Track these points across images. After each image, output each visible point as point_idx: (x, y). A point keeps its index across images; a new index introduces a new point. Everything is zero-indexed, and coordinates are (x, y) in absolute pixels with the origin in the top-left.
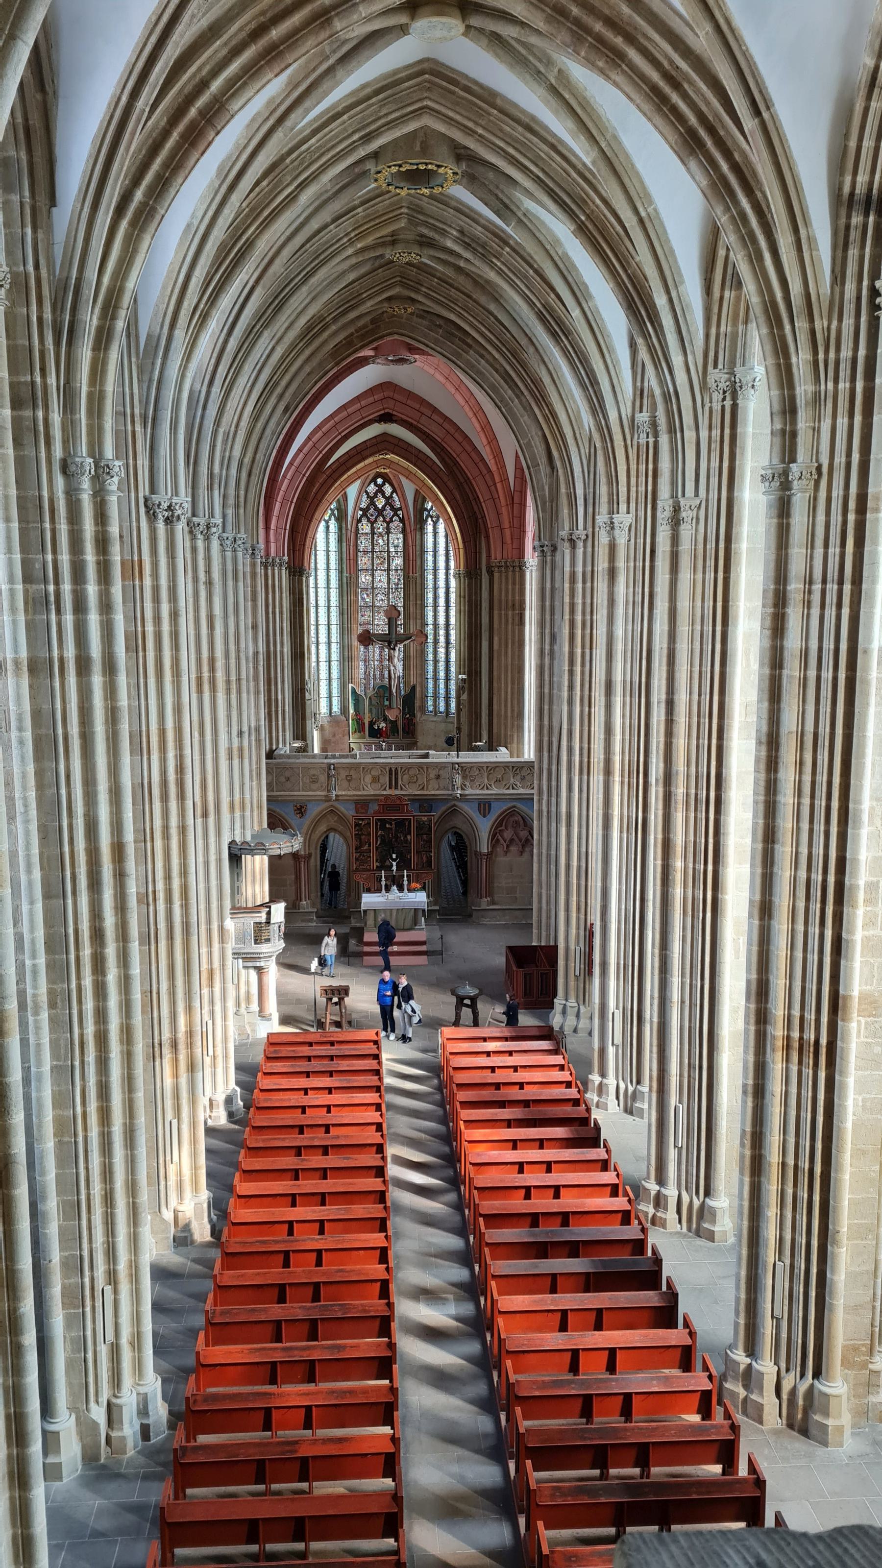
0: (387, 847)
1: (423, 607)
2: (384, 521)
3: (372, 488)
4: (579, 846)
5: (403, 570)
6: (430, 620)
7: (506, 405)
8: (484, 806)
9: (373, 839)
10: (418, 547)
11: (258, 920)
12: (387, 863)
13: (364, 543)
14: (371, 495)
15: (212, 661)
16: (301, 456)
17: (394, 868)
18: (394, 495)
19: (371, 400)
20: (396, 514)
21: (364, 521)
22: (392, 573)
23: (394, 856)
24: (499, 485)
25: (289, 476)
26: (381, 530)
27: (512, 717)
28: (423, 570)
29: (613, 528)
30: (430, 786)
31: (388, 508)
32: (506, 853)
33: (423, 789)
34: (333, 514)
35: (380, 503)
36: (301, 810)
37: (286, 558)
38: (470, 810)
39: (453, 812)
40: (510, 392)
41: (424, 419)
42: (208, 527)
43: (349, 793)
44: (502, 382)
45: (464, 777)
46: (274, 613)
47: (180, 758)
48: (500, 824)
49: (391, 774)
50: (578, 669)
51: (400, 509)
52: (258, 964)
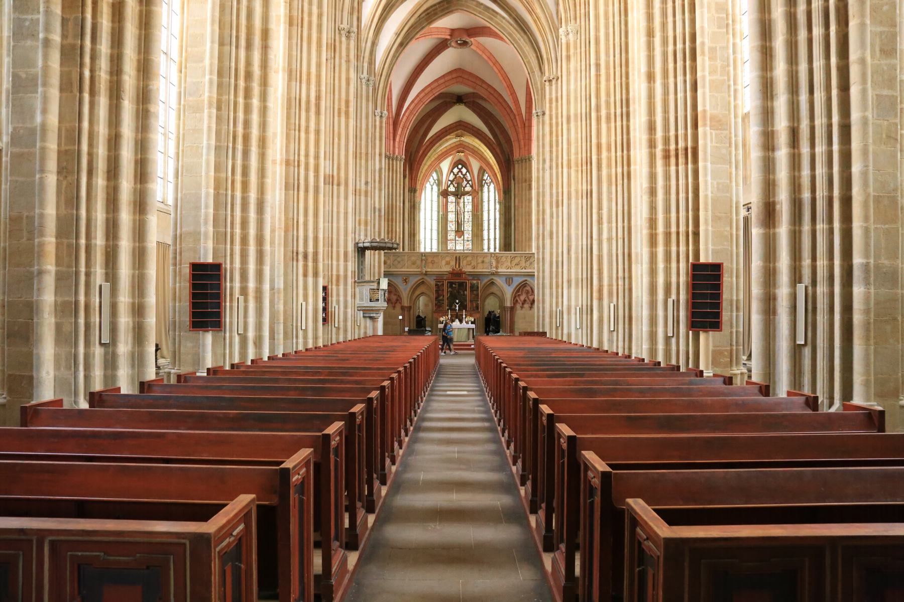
0: (453, 298)
1: (482, 230)
3: (456, 170)
4: (557, 249)
5: (473, 211)
6: (485, 237)
7: (517, 42)
8: (509, 279)
9: (445, 293)
10: (480, 199)
11: (372, 287)
12: (453, 307)
14: (456, 173)
15: (347, 102)
16: (413, 105)
17: (457, 308)
18: (468, 173)
19: (450, 77)
20: (468, 183)
21: (452, 186)
22: (466, 213)
23: (457, 301)
24: (517, 117)
25: (407, 114)
27: (526, 241)
28: (482, 211)
29: (568, 34)
30: (478, 267)
32: (522, 307)
33: (474, 268)
36: (405, 281)
37: (404, 157)
38: (500, 281)
39: (492, 283)
40: (519, 36)
41: (478, 87)
42: (349, 32)
43: (433, 270)
44: (514, 30)
45: (498, 262)
46: (396, 185)
47: (318, 92)
48: (518, 291)
49: (456, 260)
50: (554, 149)
51: (470, 181)
52: (372, 315)
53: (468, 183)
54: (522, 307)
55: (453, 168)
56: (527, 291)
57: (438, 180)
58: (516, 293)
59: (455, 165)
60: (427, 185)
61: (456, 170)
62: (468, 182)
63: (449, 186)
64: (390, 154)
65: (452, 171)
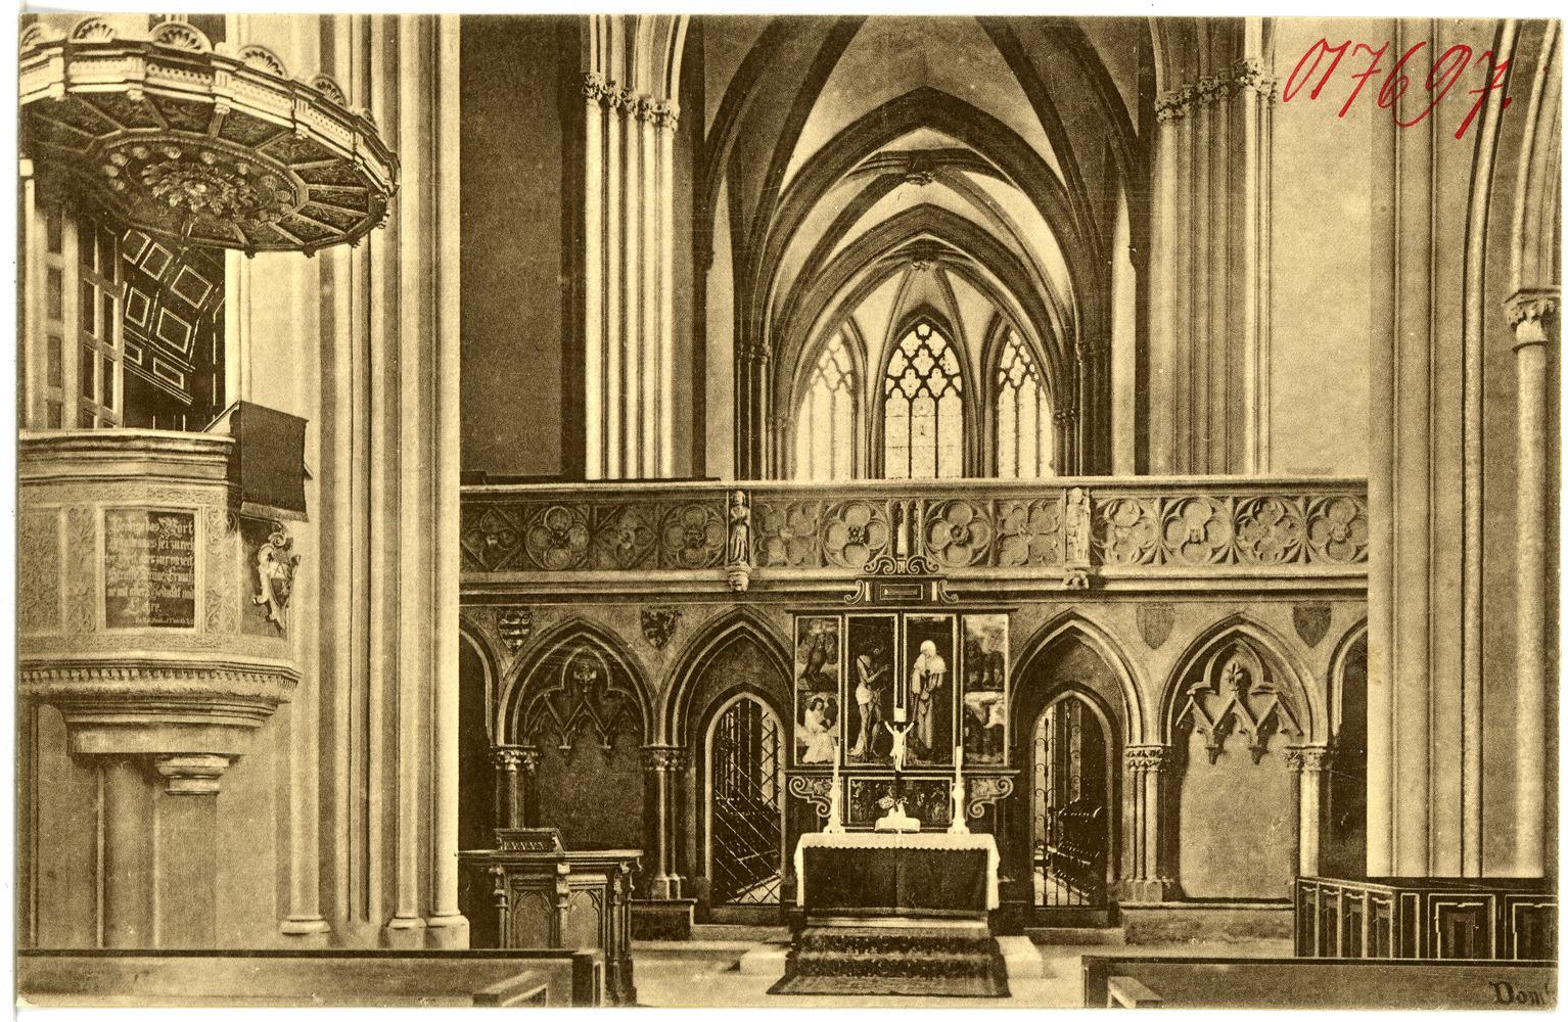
2: (931, 395)
13: (895, 430)
14: (910, 354)
21: (897, 393)
26: (924, 412)
30: (1006, 558)
31: (937, 373)
33: (983, 562)
34: (843, 380)
35: (924, 364)
45: (1099, 529)
49: (897, 522)
53: (950, 384)
54: (1216, 753)
55: (903, 337)
56: (1243, 670)
57: (854, 373)
58: (1186, 685)
59: (904, 325)
60: (816, 389)
61: (910, 342)
62: (949, 378)
63: (890, 396)
64: (610, 83)
65: (896, 346)
